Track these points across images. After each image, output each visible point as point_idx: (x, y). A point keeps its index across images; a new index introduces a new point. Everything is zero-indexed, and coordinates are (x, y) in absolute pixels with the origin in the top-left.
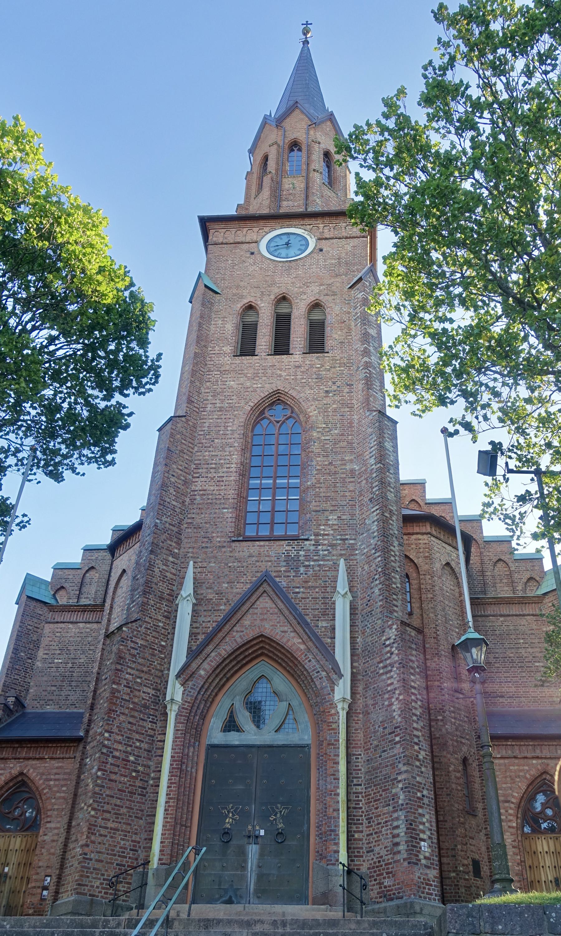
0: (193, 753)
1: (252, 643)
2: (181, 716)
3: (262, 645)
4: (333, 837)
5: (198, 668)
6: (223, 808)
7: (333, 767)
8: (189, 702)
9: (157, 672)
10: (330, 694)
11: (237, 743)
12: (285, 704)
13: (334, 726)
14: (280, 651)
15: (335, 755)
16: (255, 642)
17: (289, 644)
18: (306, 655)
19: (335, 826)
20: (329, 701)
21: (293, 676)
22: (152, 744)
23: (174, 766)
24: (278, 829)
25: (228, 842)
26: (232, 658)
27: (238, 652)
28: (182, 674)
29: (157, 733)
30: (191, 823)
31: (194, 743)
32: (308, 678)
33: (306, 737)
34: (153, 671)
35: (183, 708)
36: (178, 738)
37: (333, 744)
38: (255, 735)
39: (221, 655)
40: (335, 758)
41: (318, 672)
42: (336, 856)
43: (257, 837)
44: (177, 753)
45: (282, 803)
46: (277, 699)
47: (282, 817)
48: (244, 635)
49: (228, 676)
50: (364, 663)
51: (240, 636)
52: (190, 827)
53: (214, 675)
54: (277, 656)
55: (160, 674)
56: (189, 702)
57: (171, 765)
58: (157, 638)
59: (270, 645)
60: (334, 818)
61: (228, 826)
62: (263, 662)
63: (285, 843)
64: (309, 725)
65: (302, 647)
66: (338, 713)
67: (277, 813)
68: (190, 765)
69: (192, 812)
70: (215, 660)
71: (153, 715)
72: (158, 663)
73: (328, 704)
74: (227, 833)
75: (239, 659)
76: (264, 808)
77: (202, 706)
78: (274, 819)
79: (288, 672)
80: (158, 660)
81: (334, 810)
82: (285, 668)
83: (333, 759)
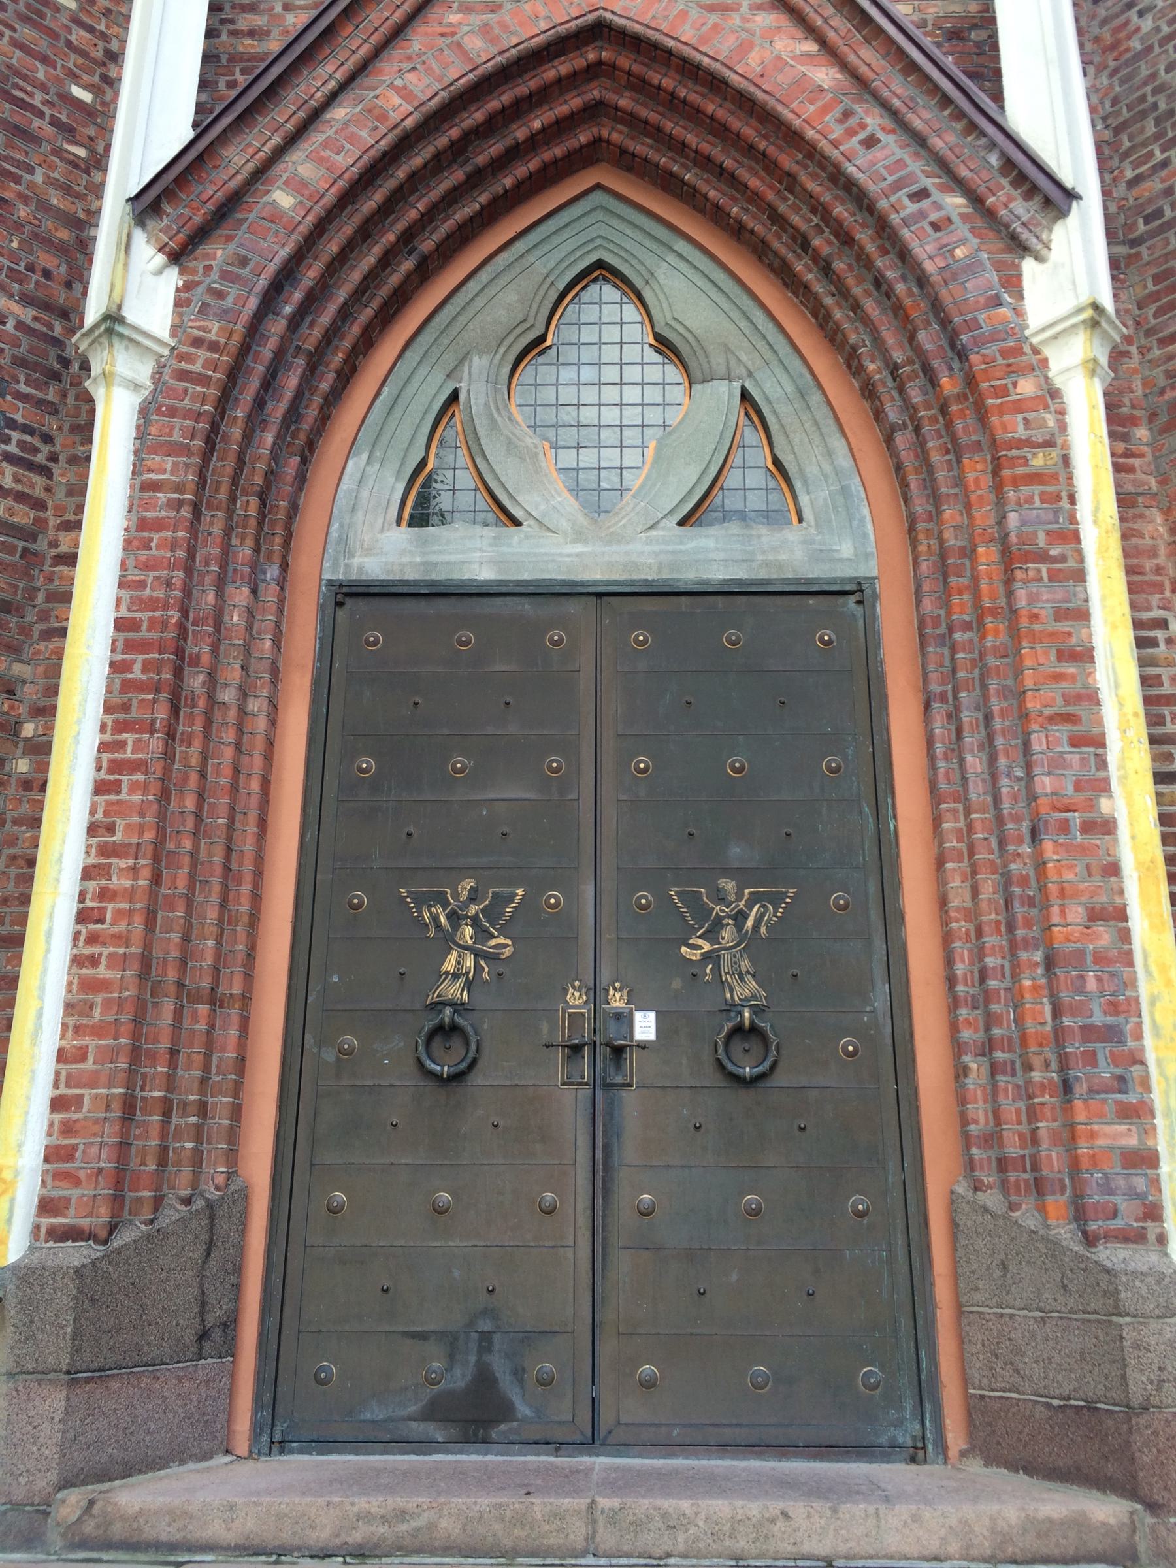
0: (250, 614)
1: (550, 73)
2: (172, 412)
3: (595, 92)
4: (1105, 1071)
5: (261, 173)
6: (422, 900)
7: (1058, 677)
8: (213, 347)
9: (48, 224)
10: (997, 302)
11: (485, 574)
12: (724, 393)
13: (1038, 461)
14: (694, 115)
15: (1061, 614)
16: (562, 67)
17: (753, 63)
18: (847, 114)
19: (1114, 1008)
20: (993, 338)
21: (760, 251)
22: (27, 575)
23: (137, 673)
24: (732, 1008)
25: (458, 1077)
26: (442, 141)
27: (476, 116)
28: (168, 194)
29: (53, 522)
30: (249, 977)
31: (255, 567)
32: (863, 236)
33: (846, 549)
34: (22, 212)
35: (183, 375)
36: (158, 525)
37: (1043, 557)
38: (579, 536)
39: (383, 117)
40: (1064, 626)
41: (923, 194)
42: (1140, 1184)
43: (618, 1051)
44: (151, 604)
45: (743, 876)
46: (673, 373)
47: (749, 942)
48: (504, 26)
49: (426, 245)
50: (1133, 183)
51: (485, 29)
52: (246, 1000)
53: (347, 228)
54: (679, 148)
55: (64, 234)
56: (213, 347)
57: (116, 667)
58: (45, 60)
59: (640, 86)
60: (1100, 958)
61: (454, 990)
62: (597, 197)
63: (780, 1079)
64: (855, 484)
65: (825, 76)
66: (1055, 394)
67: (718, 924)
68: (233, 673)
69: (254, 920)
70: (352, 139)
71: (27, 429)
72: (50, 182)
73: (992, 350)
74: (454, 1028)
75: (481, 160)
76: (645, 897)
77: (291, 381)
78: (707, 957)
79: (737, 232)
80: (53, 167)
81: (1095, 915)
82: (716, 216)
83: (1053, 635)
